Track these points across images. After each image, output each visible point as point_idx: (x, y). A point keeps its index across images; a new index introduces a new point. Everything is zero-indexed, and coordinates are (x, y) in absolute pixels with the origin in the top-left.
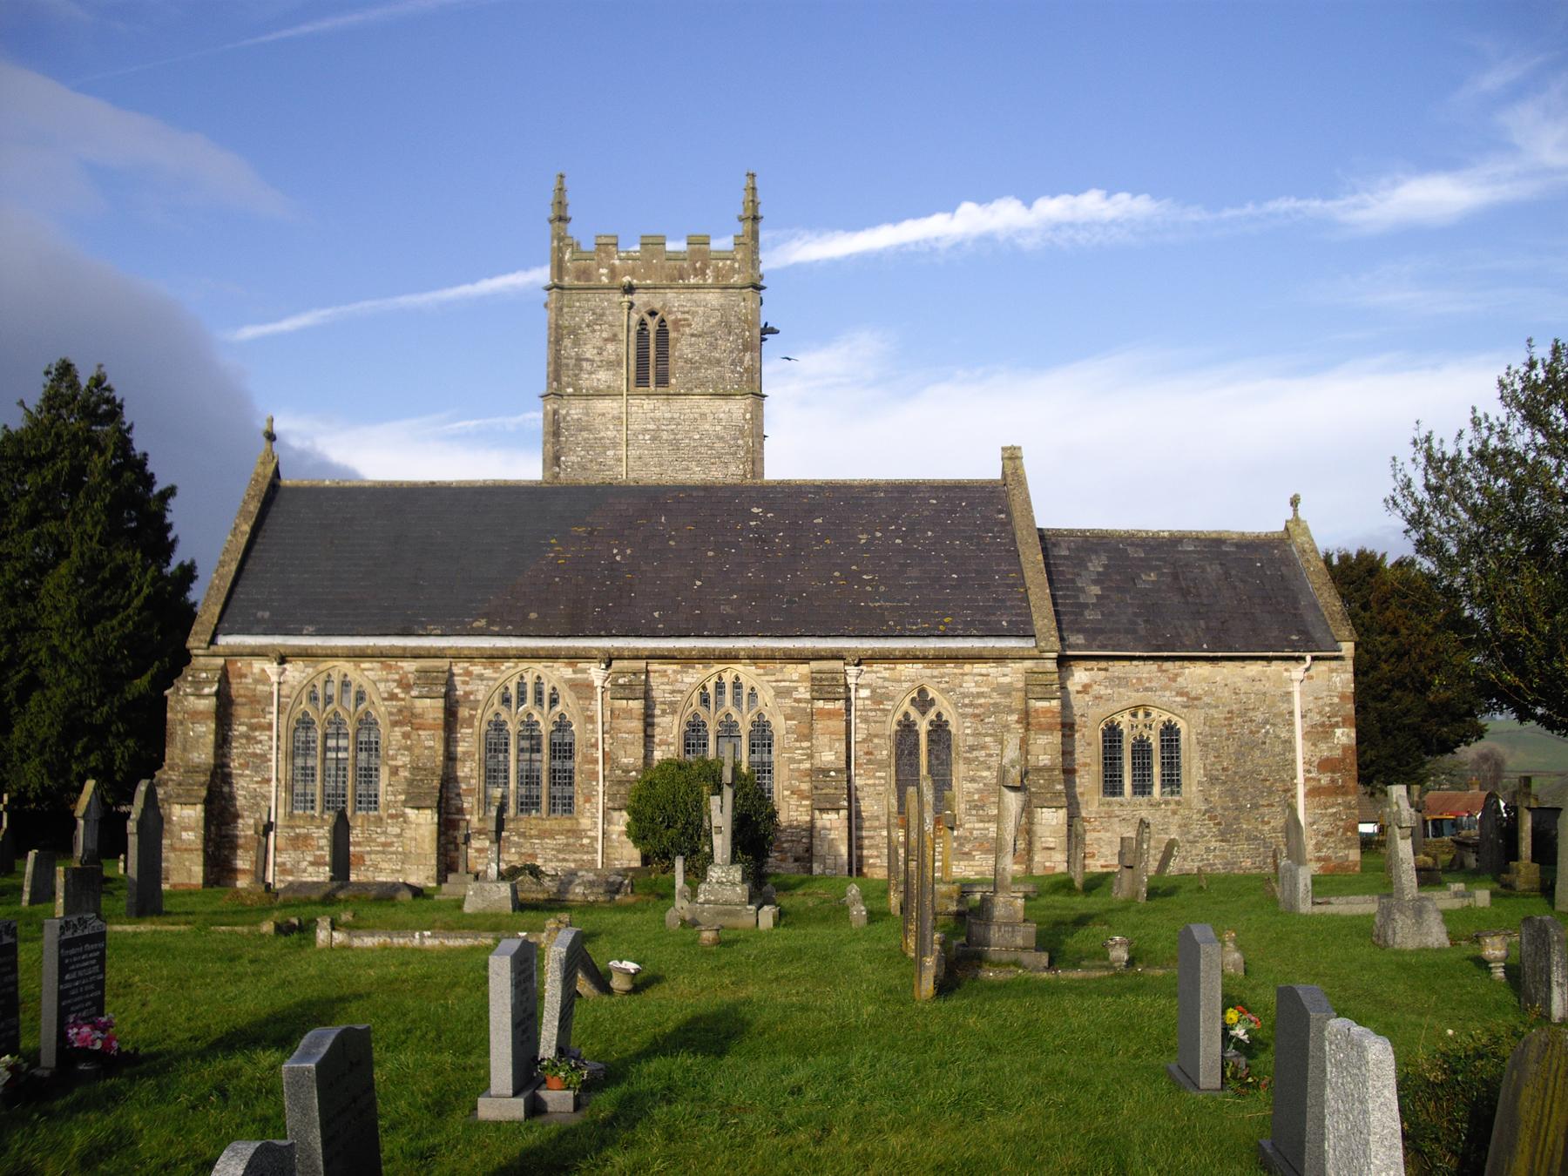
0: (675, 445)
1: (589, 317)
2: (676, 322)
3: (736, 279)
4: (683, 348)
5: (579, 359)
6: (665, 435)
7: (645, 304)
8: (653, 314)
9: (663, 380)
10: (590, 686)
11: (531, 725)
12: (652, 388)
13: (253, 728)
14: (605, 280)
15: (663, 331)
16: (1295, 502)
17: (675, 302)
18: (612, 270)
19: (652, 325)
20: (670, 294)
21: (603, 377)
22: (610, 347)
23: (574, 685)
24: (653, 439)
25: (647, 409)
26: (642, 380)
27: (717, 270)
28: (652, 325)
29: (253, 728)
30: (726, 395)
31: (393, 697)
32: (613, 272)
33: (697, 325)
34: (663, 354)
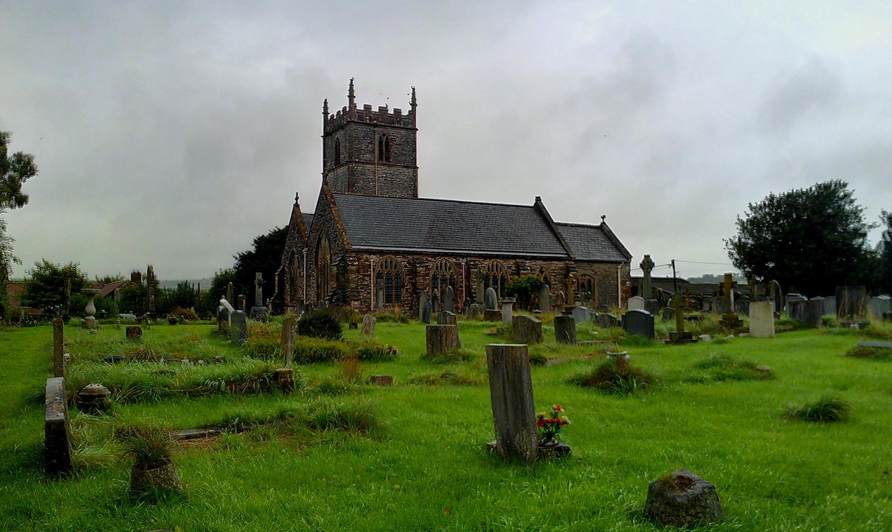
0: (392, 182)
4: (394, 149)
8: (384, 135)
9: (388, 159)
10: (460, 264)
11: (443, 276)
13: (364, 276)
16: (603, 217)
18: (371, 117)
19: (384, 139)
20: (390, 129)
22: (370, 146)
23: (456, 264)
25: (382, 171)
26: (381, 158)
29: (364, 276)
30: (407, 167)
31: (406, 266)
32: (371, 119)
33: (398, 141)
34: (388, 151)
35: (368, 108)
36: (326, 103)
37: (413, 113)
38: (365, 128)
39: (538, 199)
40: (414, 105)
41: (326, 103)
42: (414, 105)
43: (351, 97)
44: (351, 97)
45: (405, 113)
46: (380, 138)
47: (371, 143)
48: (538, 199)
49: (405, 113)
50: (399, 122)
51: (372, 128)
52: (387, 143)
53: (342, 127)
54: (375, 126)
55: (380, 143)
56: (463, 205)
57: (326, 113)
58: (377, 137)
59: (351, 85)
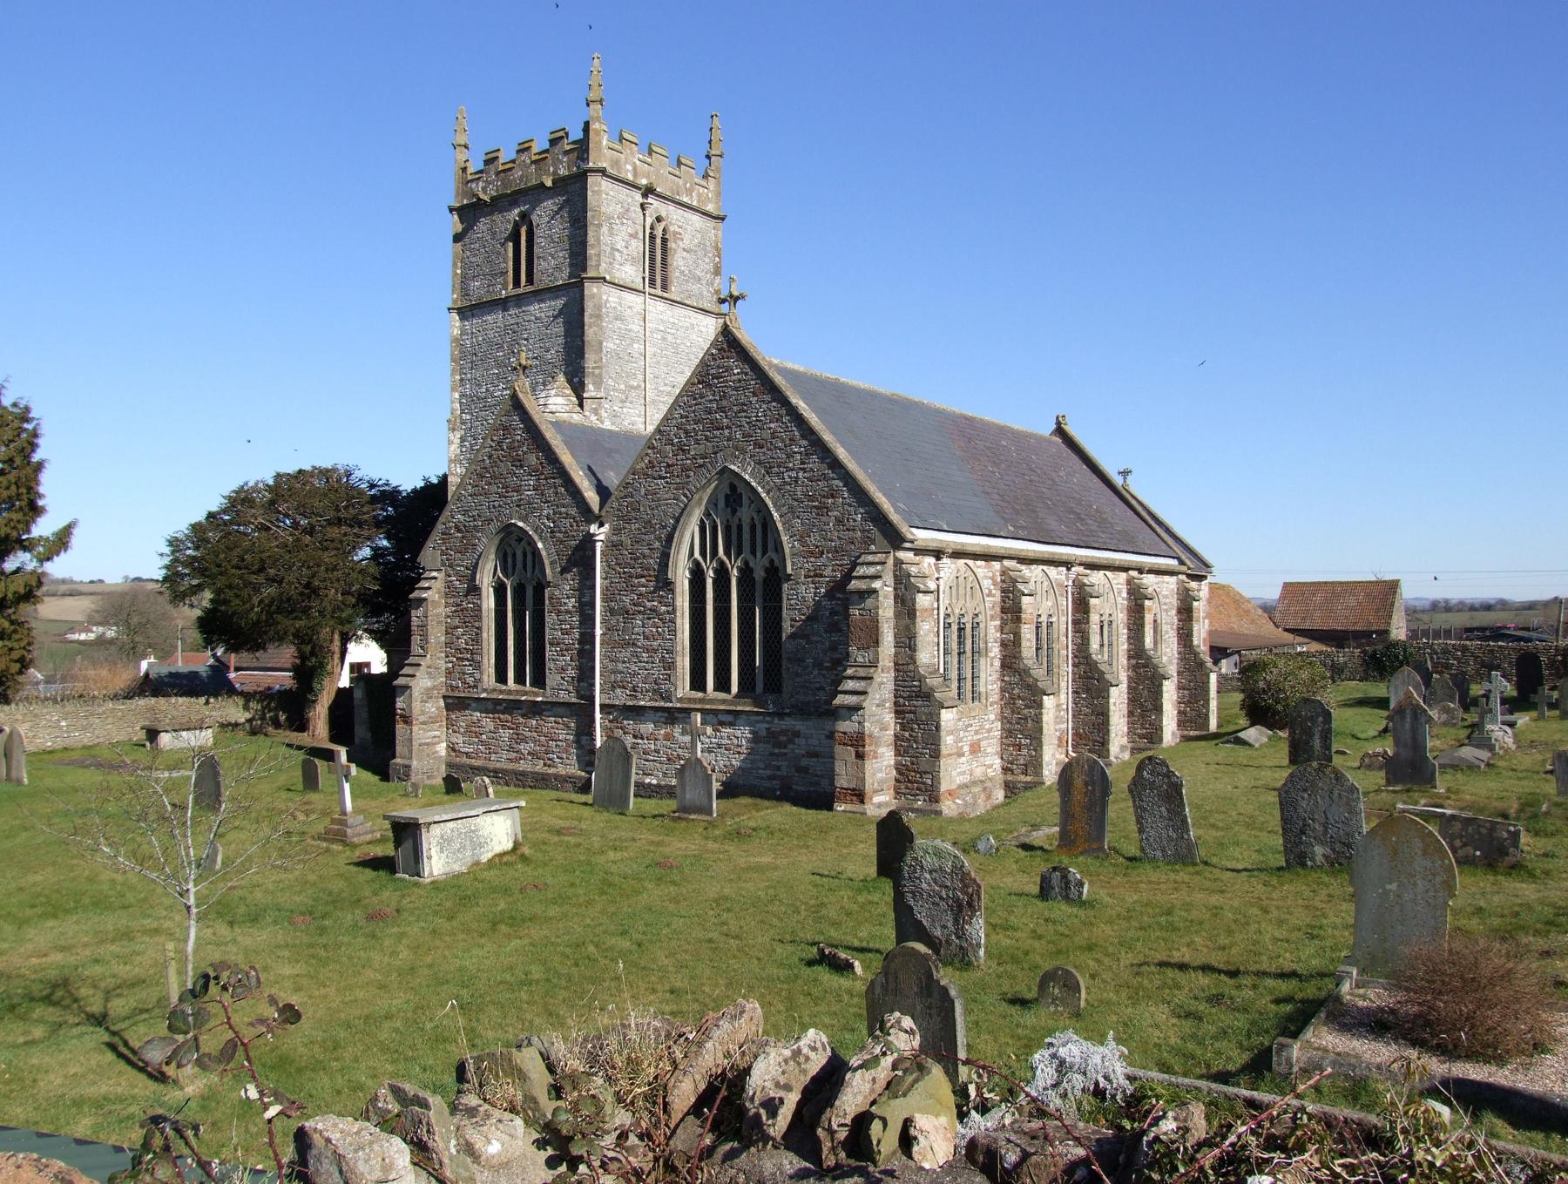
1: (619, 209)
2: (675, 233)
3: (710, 208)
5: (613, 249)
6: (670, 338)
7: (656, 210)
9: (665, 288)
14: (630, 177)
15: (665, 241)
19: (659, 233)
20: (672, 208)
22: (634, 242)
24: (664, 339)
26: (652, 282)
27: (699, 195)
28: (659, 233)
32: (635, 174)
33: (686, 243)
46: (652, 228)
47: (634, 236)
52: (665, 241)
55: (652, 237)
58: (649, 221)
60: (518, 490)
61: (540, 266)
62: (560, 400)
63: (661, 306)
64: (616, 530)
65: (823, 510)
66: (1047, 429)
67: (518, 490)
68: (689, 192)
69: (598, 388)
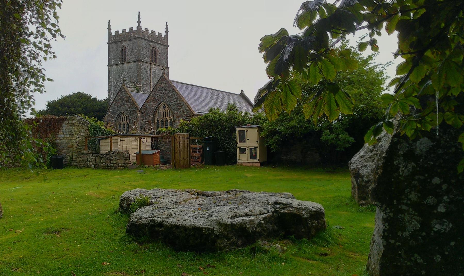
4: (158, 56)
9: (156, 62)
12: (154, 63)
17: (157, 46)
21: (147, 59)
34: (156, 57)
35: (147, 30)
36: (109, 22)
37: (166, 36)
38: (145, 42)
39: (242, 91)
40: (167, 32)
41: (109, 22)
42: (167, 32)
43: (139, 22)
44: (139, 22)
45: (163, 36)
47: (148, 51)
48: (242, 91)
49: (163, 36)
50: (161, 41)
51: (149, 42)
53: (130, 40)
54: (151, 41)
55: (152, 51)
56: (219, 92)
57: (109, 29)
59: (139, 15)
60: (124, 105)
61: (128, 57)
62: (132, 87)
63: (154, 66)
64: (142, 113)
65: (180, 109)
66: (239, 93)
67: (124, 105)
68: (161, 41)
69: (140, 84)
